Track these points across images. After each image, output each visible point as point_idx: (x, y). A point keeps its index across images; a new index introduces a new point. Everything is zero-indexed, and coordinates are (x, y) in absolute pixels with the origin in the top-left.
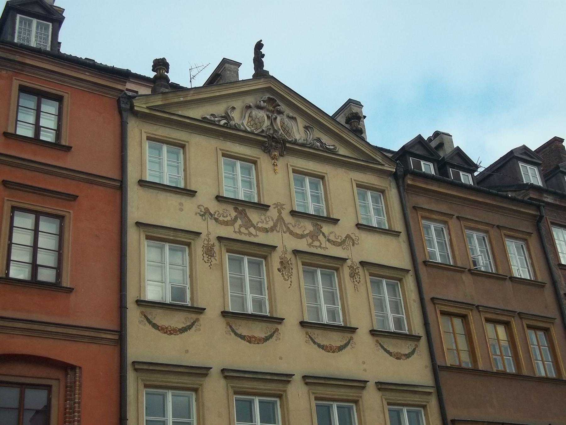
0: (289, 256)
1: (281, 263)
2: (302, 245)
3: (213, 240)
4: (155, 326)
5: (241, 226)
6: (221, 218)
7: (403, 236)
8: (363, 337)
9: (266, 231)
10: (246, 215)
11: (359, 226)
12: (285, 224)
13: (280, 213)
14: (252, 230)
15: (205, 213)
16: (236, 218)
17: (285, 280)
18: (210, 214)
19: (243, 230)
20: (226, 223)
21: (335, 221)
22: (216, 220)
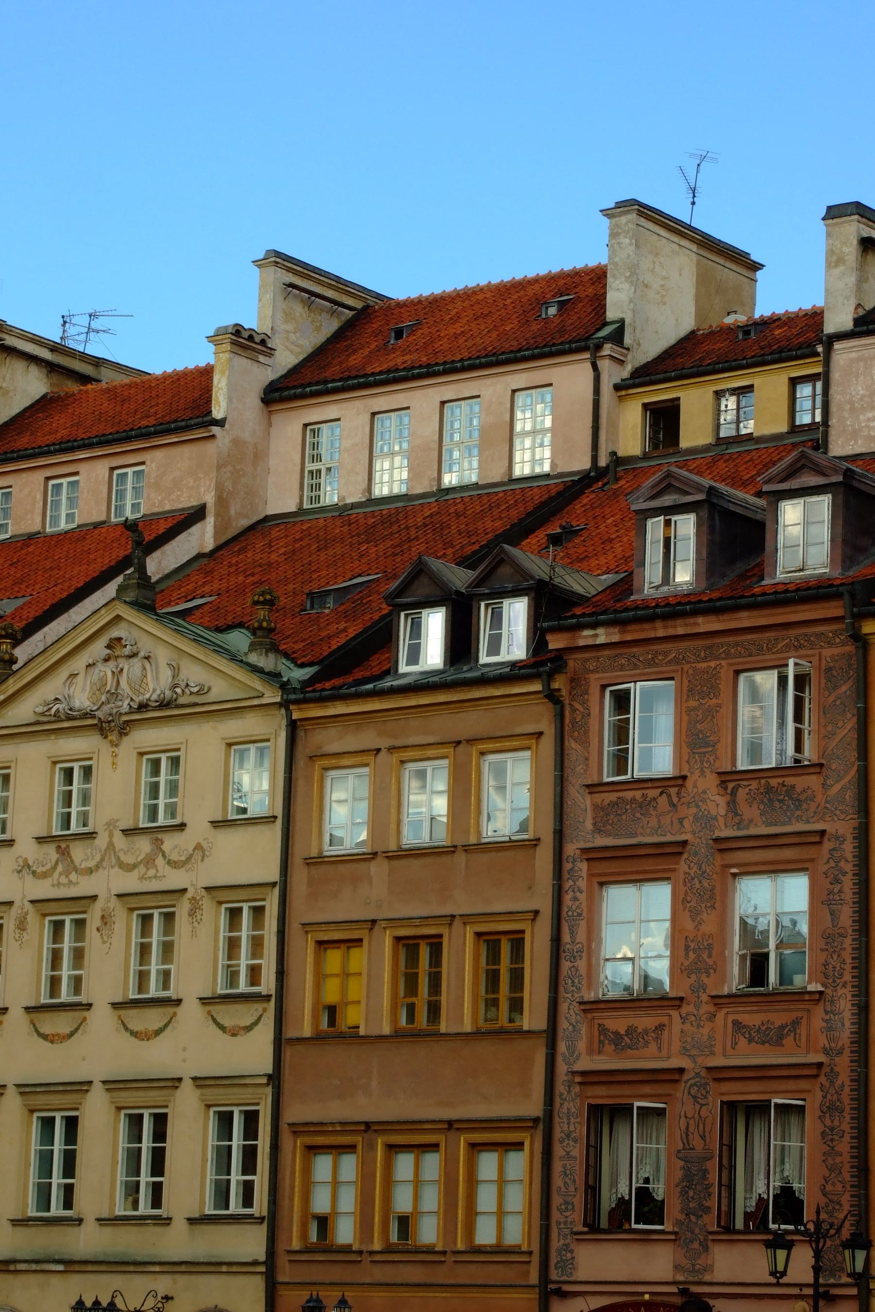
0: (114, 903)
1: (103, 917)
2: (131, 883)
5: (61, 874)
7: (279, 822)
8: (191, 1012)
9: (90, 871)
11: (216, 824)
12: (115, 852)
13: (111, 835)
14: (73, 876)
17: (104, 942)
18: (29, 867)
19: (64, 880)
20: (45, 875)
21: (182, 826)
22: (34, 873)
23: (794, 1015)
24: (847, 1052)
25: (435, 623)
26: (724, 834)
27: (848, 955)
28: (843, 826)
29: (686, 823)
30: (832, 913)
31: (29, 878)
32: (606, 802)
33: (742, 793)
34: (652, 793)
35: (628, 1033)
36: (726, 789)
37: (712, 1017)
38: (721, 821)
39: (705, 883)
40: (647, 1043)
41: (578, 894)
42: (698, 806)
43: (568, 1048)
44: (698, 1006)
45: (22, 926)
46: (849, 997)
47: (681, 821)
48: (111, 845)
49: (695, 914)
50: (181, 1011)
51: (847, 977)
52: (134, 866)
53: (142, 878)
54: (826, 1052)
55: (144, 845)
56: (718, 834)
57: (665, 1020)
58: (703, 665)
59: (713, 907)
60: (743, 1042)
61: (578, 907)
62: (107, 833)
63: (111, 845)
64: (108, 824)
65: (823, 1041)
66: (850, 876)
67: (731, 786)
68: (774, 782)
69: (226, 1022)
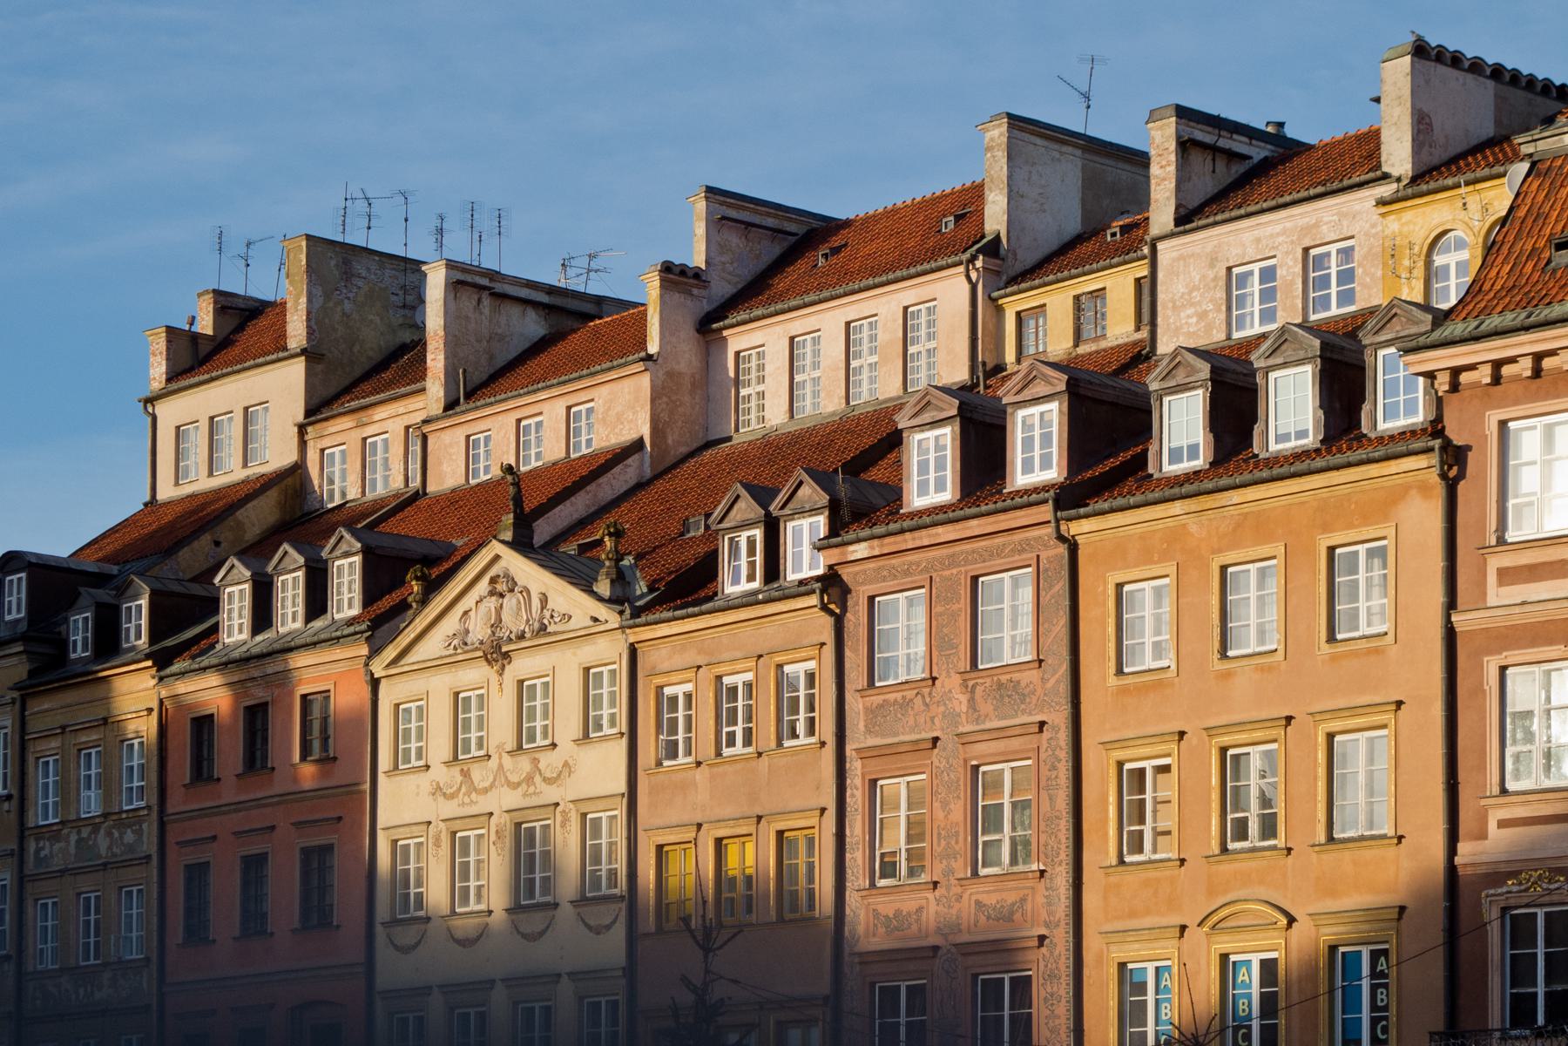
9: (486, 791)
14: (474, 796)
15: (438, 790)
19: (467, 800)
20: (452, 796)
23: (1022, 893)
24: (1063, 923)
26: (965, 730)
28: (1059, 717)
31: (441, 799)
33: (979, 690)
34: (910, 694)
38: (964, 717)
44: (948, 889)
47: (932, 719)
48: (501, 766)
51: (1063, 856)
52: (519, 784)
53: (525, 795)
54: (1047, 925)
55: (524, 763)
56: (961, 729)
58: (947, 573)
63: (501, 766)
66: (1063, 762)
67: (971, 683)
68: (1004, 678)
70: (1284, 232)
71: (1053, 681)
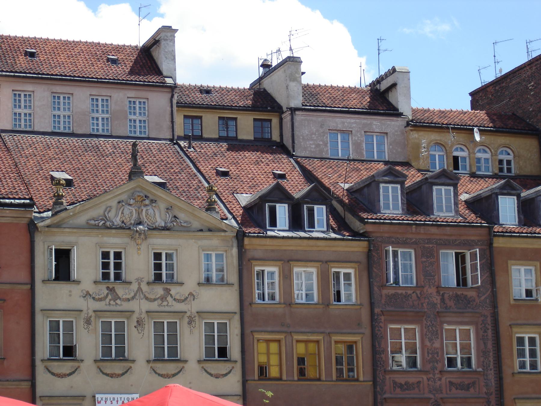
0: (144, 315)
1: (138, 321)
2: (154, 306)
3: (91, 313)
4: (53, 374)
5: (110, 300)
6: (97, 297)
7: (236, 287)
9: (128, 300)
10: (114, 290)
12: (142, 292)
13: (139, 284)
14: (118, 301)
15: (87, 295)
16: (107, 295)
17: (139, 333)
18: (90, 295)
19: (112, 302)
20: (100, 300)
21: (182, 284)
22: (94, 298)
25: (282, 211)
27: (491, 359)
29: (424, 305)
30: (485, 343)
31: (91, 301)
32: (390, 294)
35: (405, 384)
36: (440, 293)
37: (440, 379)
38: (439, 306)
39: (434, 329)
40: (414, 389)
41: (380, 329)
42: (428, 299)
43: (380, 389)
44: (434, 375)
45: (88, 321)
46: (493, 374)
47: (422, 304)
48: (140, 289)
49: (431, 340)
50: (186, 366)
51: (492, 366)
53: (160, 305)
55: (159, 290)
57: (421, 379)
58: (427, 246)
59: (437, 338)
60: (454, 389)
61: (381, 334)
62: (137, 283)
63: (140, 289)
64: (137, 279)
65: (485, 390)
66: (490, 330)
69: (213, 372)
70: (355, 123)
71: (483, 298)
